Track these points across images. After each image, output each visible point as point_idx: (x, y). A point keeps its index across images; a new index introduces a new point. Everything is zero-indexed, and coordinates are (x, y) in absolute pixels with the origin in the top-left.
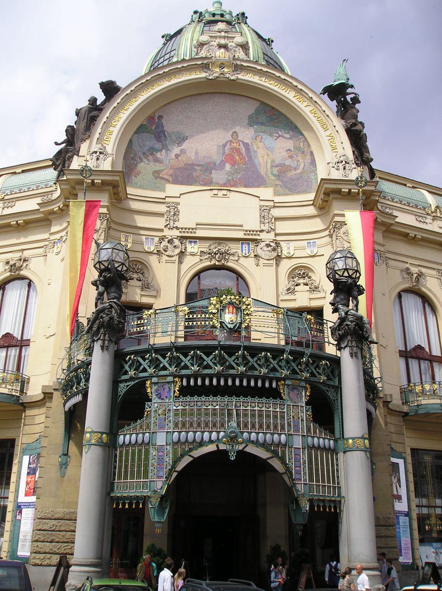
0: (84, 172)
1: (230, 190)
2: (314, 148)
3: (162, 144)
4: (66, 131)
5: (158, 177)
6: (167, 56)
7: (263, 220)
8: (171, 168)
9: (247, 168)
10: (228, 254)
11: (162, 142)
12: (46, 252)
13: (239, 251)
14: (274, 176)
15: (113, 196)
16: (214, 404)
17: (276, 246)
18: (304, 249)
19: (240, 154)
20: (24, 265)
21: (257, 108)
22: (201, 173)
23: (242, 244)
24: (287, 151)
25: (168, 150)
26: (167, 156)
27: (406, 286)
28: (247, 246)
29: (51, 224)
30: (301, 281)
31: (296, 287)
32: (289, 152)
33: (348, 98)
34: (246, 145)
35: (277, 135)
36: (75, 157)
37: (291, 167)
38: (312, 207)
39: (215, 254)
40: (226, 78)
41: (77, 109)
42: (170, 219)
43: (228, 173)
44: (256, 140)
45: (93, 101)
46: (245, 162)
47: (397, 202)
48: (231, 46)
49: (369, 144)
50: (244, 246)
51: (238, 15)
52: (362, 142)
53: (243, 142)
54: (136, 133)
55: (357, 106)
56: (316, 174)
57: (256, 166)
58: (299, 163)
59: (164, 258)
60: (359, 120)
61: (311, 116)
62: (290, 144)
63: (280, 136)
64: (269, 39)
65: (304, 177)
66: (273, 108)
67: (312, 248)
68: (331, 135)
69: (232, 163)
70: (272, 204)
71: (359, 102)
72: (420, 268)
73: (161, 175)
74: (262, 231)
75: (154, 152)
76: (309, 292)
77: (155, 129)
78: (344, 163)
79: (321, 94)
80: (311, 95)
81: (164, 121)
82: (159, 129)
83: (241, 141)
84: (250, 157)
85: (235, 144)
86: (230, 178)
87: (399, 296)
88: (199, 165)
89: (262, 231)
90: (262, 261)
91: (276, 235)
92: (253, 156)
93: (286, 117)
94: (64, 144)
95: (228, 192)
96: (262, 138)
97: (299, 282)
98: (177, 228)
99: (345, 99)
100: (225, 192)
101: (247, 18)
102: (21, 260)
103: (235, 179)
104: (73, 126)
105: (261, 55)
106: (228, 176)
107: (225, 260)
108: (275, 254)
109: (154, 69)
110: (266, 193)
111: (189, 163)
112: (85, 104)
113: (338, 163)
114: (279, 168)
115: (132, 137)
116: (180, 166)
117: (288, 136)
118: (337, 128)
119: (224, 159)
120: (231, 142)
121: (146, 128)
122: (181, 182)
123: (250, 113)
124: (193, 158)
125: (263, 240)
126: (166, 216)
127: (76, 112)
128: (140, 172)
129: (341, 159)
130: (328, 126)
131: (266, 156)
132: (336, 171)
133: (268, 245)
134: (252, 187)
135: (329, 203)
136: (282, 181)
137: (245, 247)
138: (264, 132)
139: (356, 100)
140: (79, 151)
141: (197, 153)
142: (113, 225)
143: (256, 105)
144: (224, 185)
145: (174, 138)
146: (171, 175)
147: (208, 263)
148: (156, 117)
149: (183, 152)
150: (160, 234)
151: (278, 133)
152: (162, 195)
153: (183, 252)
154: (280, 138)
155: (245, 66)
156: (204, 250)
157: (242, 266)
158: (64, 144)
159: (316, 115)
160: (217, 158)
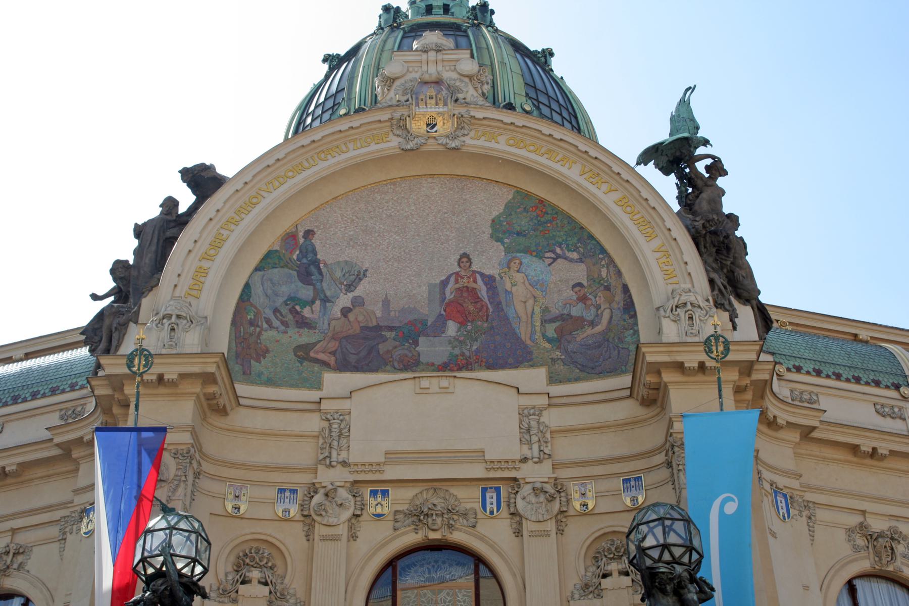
0: (136, 361)
1: (455, 377)
2: (629, 278)
3: (315, 289)
4: (112, 271)
5: (304, 359)
7: (527, 437)
8: (333, 338)
9: (492, 328)
10: (454, 514)
11: (314, 285)
12: (65, 533)
13: (478, 506)
14: (549, 341)
15: (205, 404)
18: (616, 495)
19: (476, 299)
20: (15, 566)
21: (509, 202)
22: (398, 343)
23: (484, 490)
24: (574, 286)
25: (326, 300)
26: (324, 315)
27: (865, 565)
28: (494, 495)
29: (77, 470)
30: (614, 567)
31: (603, 581)
32: (577, 289)
33: (701, 166)
34: (490, 281)
35: (553, 256)
36: (132, 325)
37: (585, 320)
38: (630, 402)
39: (427, 515)
40: (442, 144)
41: (136, 225)
42: (330, 447)
44: (509, 268)
45: (170, 204)
46: (488, 316)
47: (828, 377)
48: (451, 79)
49: (752, 259)
50: (488, 495)
51: (474, 8)
52: (735, 258)
53: (482, 275)
54: (257, 269)
55: (721, 182)
56: (636, 332)
57: (510, 323)
58: (599, 312)
59: (320, 530)
60: (726, 210)
61: (617, 210)
62: (580, 273)
63: (559, 256)
64: (543, 50)
65: (611, 340)
66: (541, 201)
67: (634, 493)
68: (663, 249)
69: (461, 320)
71: (725, 173)
72: (894, 523)
73: (312, 354)
74: (524, 460)
75: (298, 308)
76: (630, 589)
77: (298, 259)
78: (689, 307)
79: (638, 164)
80: (616, 169)
81: (317, 241)
82: (306, 257)
83: (478, 272)
84: (498, 305)
85: (465, 280)
86: (457, 351)
87: (851, 588)
88: (391, 329)
89: (524, 460)
90: (527, 526)
91: (555, 467)
92: (504, 303)
93: (571, 219)
94: (112, 298)
95: (452, 379)
96: (521, 263)
97: (609, 568)
98: (345, 464)
99: (694, 169)
100: (445, 383)
101: (492, 12)
102: (8, 553)
103: (467, 354)
104: (127, 261)
105: (520, 88)
106: (453, 348)
107: (449, 528)
108: (556, 506)
109: (304, 128)
110: (533, 378)
111: (370, 325)
112: (154, 211)
113: (677, 307)
114: (557, 324)
115: (249, 277)
116: (351, 332)
117: (575, 255)
118: (674, 234)
119: (443, 312)
120: (457, 274)
121: (280, 258)
122: (355, 367)
123: (495, 214)
124: (379, 314)
125: (527, 480)
126: (321, 441)
127: (135, 231)
128: (267, 351)
129: (684, 298)
130: (656, 228)
131: (531, 302)
132: (672, 323)
133: (537, 491)
134: (503, 367)
135: (661, 394)
136: (566, 352)
137: (491, 497)
138: (527, 251)
139: (717, 168)
140: (137, 313)
141: (386, 303)
142: (206, 467)
143: (508, 195)
144: (444, 367)
145: (338, 274)
146: (333, 353)
147: (411, 538)
148: (301, 234)
149: (358, 302)
150: (307, 478)
151: (554, 252)
152: (314, 395)
153: (358, 516)
154: (559, 260)
155: (479, 119)
156: (404, 507)
157: (482, 538)
158: (112, 298)
159: (629, 209)
160: (429, 311)
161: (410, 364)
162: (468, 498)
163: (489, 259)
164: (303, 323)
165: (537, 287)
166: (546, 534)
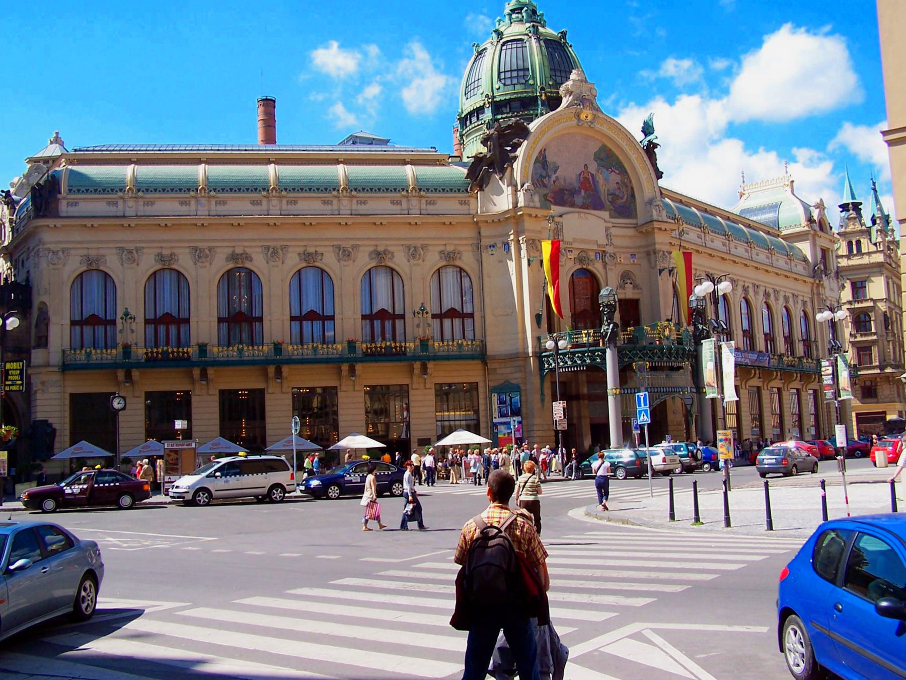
6: (521, 73)
16: (662, 375)
17: (613, 256)
25: (549, 177)
30: (629, 281)
34: (592, 175)
43: (584, 197)
62: (618, 178)
70: (610, 225)
90: (608, 267)
93: (618, 158)
110: (605, 214)
144: (581, 207)
147: (579, 267)
149: (557, 178)
160: (576, 185)
161: (573, 205)
162: (592, 256)
163: (593, 168)
164: (545, 186)
165: (607, 182)
166: (611, 269)
